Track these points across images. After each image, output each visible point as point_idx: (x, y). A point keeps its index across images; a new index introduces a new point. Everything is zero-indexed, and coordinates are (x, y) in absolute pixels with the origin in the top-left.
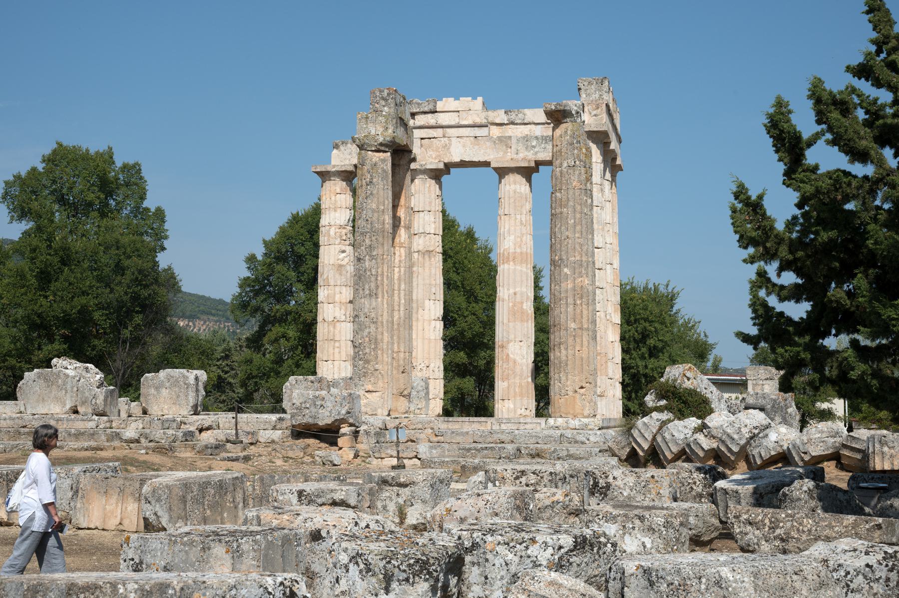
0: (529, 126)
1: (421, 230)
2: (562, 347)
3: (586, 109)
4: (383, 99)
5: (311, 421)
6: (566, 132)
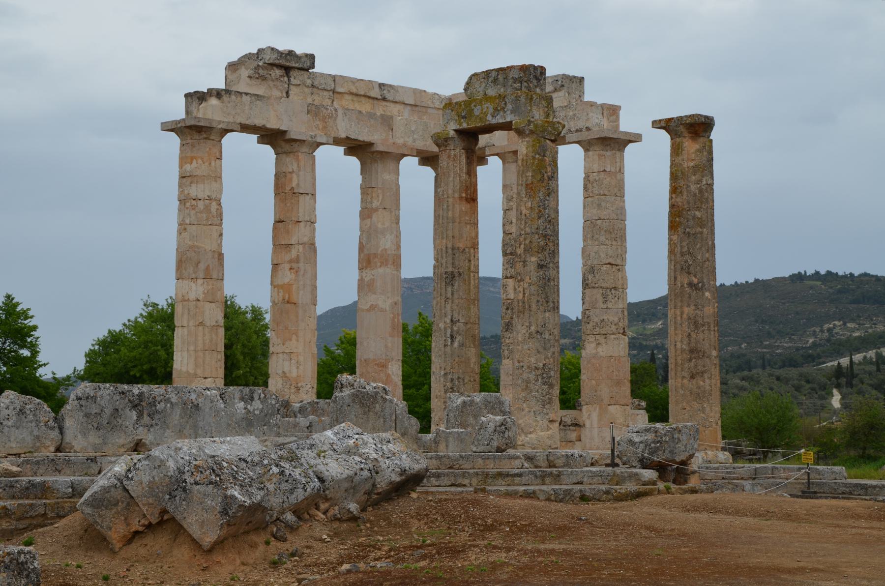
0: (398, 106)
1: (307, 218)
2: (706, 375)
3: (605, 114)
4: (536, 77)
5: (669, 456)
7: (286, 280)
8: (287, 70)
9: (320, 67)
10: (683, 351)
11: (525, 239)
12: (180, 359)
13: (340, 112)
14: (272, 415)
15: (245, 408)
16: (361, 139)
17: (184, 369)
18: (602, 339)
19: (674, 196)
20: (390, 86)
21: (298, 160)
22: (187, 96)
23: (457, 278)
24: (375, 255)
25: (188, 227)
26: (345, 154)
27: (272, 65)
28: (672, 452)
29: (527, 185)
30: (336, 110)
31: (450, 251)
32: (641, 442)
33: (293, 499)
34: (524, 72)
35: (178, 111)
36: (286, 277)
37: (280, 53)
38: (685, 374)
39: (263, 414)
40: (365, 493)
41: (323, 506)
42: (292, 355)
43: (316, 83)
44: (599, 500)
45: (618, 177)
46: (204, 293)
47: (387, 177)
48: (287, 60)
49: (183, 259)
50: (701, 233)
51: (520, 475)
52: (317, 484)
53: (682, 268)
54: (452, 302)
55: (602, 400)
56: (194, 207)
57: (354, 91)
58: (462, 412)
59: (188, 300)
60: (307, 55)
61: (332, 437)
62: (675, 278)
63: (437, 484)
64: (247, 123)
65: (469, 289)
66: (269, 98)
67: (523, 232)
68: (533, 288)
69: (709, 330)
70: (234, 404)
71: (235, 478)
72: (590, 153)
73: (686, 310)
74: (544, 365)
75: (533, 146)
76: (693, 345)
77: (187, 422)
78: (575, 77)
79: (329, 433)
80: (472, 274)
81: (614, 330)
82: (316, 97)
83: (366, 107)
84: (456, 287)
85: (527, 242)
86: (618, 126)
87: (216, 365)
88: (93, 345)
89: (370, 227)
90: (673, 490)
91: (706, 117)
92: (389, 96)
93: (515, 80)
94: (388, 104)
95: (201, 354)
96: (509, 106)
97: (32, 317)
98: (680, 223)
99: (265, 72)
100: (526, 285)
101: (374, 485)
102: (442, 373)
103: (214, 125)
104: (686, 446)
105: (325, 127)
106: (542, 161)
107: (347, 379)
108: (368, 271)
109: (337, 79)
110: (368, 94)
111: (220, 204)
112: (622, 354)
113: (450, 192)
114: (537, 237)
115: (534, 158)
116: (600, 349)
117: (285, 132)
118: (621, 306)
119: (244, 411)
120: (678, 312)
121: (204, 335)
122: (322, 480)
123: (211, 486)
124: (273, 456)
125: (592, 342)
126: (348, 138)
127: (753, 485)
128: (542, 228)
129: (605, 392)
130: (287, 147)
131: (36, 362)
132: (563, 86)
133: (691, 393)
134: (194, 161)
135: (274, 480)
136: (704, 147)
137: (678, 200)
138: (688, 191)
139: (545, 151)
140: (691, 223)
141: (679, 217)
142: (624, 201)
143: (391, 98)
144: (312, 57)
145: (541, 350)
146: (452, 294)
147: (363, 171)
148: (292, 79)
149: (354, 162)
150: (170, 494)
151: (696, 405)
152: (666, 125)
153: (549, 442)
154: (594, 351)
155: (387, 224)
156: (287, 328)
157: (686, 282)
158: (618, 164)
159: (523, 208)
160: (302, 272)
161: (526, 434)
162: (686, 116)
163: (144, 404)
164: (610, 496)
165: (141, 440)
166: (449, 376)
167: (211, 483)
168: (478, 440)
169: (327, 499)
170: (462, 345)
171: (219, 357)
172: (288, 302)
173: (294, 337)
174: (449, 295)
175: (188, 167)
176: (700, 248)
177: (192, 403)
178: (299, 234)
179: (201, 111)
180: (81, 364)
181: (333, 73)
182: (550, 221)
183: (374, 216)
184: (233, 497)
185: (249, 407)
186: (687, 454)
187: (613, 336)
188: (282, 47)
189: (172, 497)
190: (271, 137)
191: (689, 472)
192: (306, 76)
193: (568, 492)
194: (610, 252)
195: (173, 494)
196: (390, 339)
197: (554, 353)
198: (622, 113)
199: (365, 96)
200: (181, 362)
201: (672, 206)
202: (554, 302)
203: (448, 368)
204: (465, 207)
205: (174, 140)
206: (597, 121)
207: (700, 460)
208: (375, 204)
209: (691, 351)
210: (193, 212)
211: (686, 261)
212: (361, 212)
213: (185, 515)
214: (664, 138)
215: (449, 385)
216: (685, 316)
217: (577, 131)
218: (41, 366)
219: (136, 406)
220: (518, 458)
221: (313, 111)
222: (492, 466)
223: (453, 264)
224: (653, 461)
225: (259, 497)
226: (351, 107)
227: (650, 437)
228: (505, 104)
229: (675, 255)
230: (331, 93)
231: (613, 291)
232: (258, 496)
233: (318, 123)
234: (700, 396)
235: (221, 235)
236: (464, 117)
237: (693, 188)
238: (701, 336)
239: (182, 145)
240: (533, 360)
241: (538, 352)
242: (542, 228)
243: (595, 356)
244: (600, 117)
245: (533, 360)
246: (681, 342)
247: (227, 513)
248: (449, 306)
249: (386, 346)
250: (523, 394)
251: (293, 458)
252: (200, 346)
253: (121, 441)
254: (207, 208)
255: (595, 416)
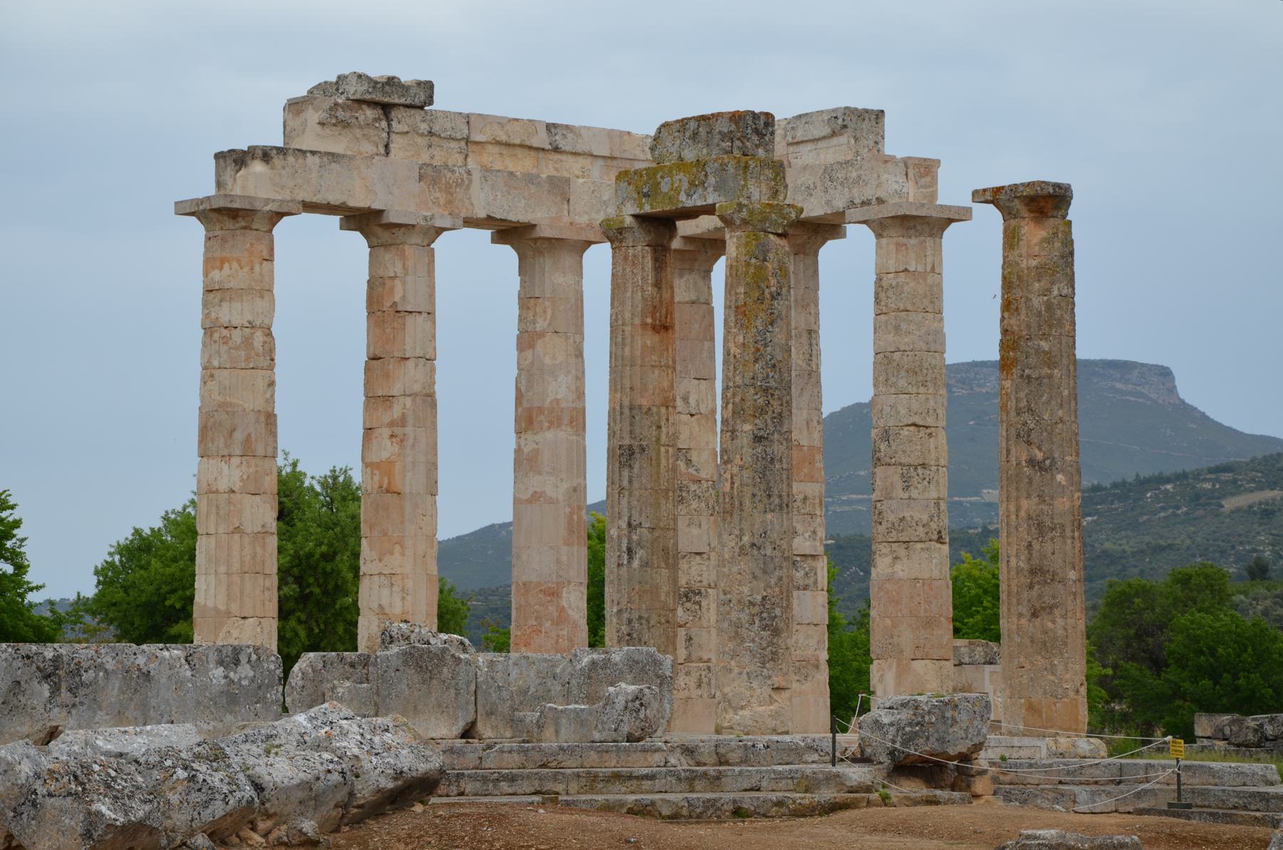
0: (580, 159)
1: (419, 352)
4: (757, 132)
6: (1055, 234)
7: (385, 455)
8: (386, 109)
9: (441, 103)
10: (1019, 571)
11: (734, 395)
12: (204, 587)
13: (476, 176)
14: (270, 686)
15: (226, 677)
16: (513, 217)
17: (210, 604)
18: (901, 551)
19: (1006, 315)
20: (567, 127)
21: (403, 256)
22: (219, 156)
23: (637, 455)
24: (540, 410)
25: (216, 372)
26: (493, 241)
27: (360, 102)
28: (941, 740)
29: (737, 307)
30: (469, 173)
31: (626, 411)
32: (892, 724)
33: (207, 815)
34: (737, 123)
35: (204, 186)
36: (385, 449)
37: (374, 83)
38: (1024, 609)
39: (255, 685)
40: (336, 806)
41: (263, 825)
42: (394, 578)
43: (436, 129)
44: (765, 816)
45: (930, 280)
46: (242, 480)
47: (559, 279)
48: (384, 93)
49: (210, 424)
50: (1050, 377)
51: (651, 777)
52: (249, 792)
53: (1018, 435)
54: (630, 495)
55: (902, 652)
56: (225, 340)
57: (503, 138)
58: (590, 678)
59: (217, 492)
60: (419, 83)
61: (305, 723)
62: (1008, 451)
63: (510, 790)
64: (314, 200)
65: (658, 473)
66: (351, 158)
67: (731, 384)
68: (746, 474)
69: (1063, 536)
70: (207, 670)
71: (109, 787)
72: (884, 241)
73: (1025, 504)
74: (764, 598)
75: (747, 244)
76: (1035, 561)
77: (131, 699)
78: (867, 111)
79: (301, 718)
80: (663, 449)
81: (922, 535)
82: (436, 152)
83: (523, 164)
84: (635, 470)
85: (737, 399)
86: (934, 195)
87: (263, 596)
88: (111, 554)
89: (532, 363)
90: (894, 800)
91: (1057, 186)
92: (564, 145)
93: (723, 136)
94: (564, 157)
95: (236, 579)
96: (712, 180)
97: (12, 507)
98: (1015, 361)
99: (348, 114)
100: (736, 470)
101: (351, 794)
102: (615, 610)
103: (258, 206)
104: (966, 730)
105: (450, 202)
106: (760, 268)
107: (400, 629)
108: (529, 436)
109: (472, 119)
110: (528, 143)
111: (270, 334)
112: (936, 574)
113: (627, 315)
114: (752, 391)
115: (748, 264)
116: (898, 567)
117: (379, 213)
118: (934, 494)
119: (223, 681)
120: (1012, 508)
121: (242, 548)
122: (259, 788)
123: (69, 799)
124: (183, 755)
125: (886, 555)
126: (490, 218)
127: (1093, 793)
128: (760, 376)
129: (906, 639)
130: (385, 236)
131: (20, 584)
132: (845, 127)
133: (1032, 641)
134: (226, 265)
135: (180, 788)
136: (1055, 234)
137: (1013, 322)
138: (1028, 308)
139: (765, 253)
140: (1032, 360)
141: (1013, 349)
142: (942, 319)
143: (568, 148)
144: (428, 87)
145: (758, 573)
146: (630, 482)
147: (522, 270)
148: (394, 124)
149: (507, 255)
150: (15, 810)
151: (1041, 662)
152: (995, 196)
153: (772, 723)
154: (890, 570)
155: (560, 359)
156: (386, 534)
157: (1024, 457)
158: (929, 259)
159: (731, 345)
160: (411, 441)
161: (736, 709)
162: (1023, 184)
163: (60, 672)
164: (784, 810)
165: (57, 727)
166: (626, 615)
167: (69, 794)
168: (603, 723)
169: (269, 816)
170: (645, 564)
171: (268, 583)
172: (388, 491)
173: (397, 547)
174: (625, 483)
175: (216, 275)
176: (1048, 402)
177: (139, 670)
178: (406, 379)
179: (239, 182)
180: (90, 590)
181: (467, 112)
182: (774, 366)
183: (539, 344)
184: (99, 814)
185: (232, 674)
186: (969, 744)
187: (919, 546)
188: (377, 71)
189: (18, 814)
190: (361, 220)
191: (973, 772)
192: (418, 118)
193: (711, 804)
194: (915, 406)
195: (19, 810)
196: (565, 548)
197: (780, 579)
198: (941, 172)
199: (522, 146)
200: (207, 592)
201: (1005, 332)
202: (780, 496)
203: (624, 601)
204: (651, 339)
205: (195, 230)
206: (895, 186)
207: (1044, 751)
208: (541, 325)
209: (1033, 572)
210: (225, 348)
211: (1025, 424)
212: (519, 338)
213: (35, 839)
214: (990, 220)
215: (625, 629)
216: (1022, 514)
217: (863, 203)
218: (31, 589)
219: (49, 676)
220: (659, 750)
221: (429, 175)
222: (613, 763)
223: (631, 432)
224: (909, 755)
225: (141, 814)
226: (498, 165)
227: (905, 715)
228: (706, 175)
229: (1008, 413)
230: (463, 144)
231: (920, 471)
232: (140, 811)
233: (438, 195)
234: (1048, 646)
235: (272, 384)
236: (646, 195)
237: (1037, 302)
238: (1049, 547)
239: (208, 239)
240: (746, 590)
241: (755, 577)
242: (760, 376)
243: (890, 578)
244: (902, 179)
245: (746, 590)
246: (1017, 556)
247: (91, 837)
248: (624, 502)
249: (558, 561)
250: (731, 645)
251: (217, 757)
252: (236, 566)
253: (25, 729)
254: (247, 342)
255: (890, 678)
